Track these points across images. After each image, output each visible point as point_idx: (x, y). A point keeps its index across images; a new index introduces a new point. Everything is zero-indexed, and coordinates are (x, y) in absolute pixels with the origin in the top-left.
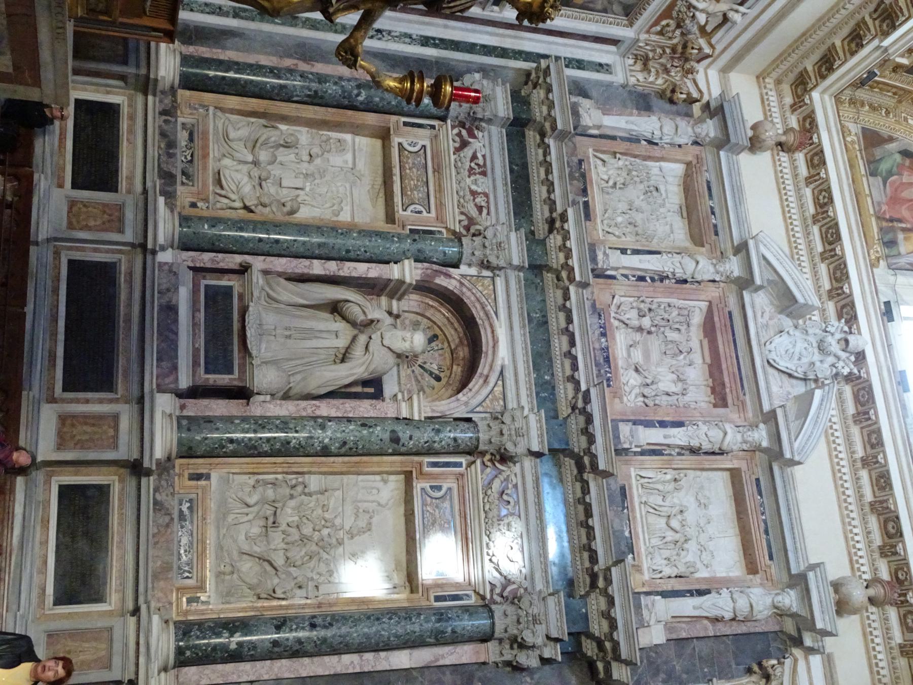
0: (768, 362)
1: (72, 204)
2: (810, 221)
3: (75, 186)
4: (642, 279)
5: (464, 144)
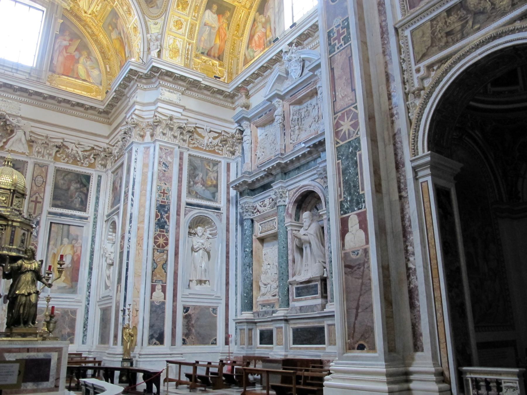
0: (300, 76)
1: (278, 344)
2: (264, 77)
3: (272, 343)
5: (258, 211)
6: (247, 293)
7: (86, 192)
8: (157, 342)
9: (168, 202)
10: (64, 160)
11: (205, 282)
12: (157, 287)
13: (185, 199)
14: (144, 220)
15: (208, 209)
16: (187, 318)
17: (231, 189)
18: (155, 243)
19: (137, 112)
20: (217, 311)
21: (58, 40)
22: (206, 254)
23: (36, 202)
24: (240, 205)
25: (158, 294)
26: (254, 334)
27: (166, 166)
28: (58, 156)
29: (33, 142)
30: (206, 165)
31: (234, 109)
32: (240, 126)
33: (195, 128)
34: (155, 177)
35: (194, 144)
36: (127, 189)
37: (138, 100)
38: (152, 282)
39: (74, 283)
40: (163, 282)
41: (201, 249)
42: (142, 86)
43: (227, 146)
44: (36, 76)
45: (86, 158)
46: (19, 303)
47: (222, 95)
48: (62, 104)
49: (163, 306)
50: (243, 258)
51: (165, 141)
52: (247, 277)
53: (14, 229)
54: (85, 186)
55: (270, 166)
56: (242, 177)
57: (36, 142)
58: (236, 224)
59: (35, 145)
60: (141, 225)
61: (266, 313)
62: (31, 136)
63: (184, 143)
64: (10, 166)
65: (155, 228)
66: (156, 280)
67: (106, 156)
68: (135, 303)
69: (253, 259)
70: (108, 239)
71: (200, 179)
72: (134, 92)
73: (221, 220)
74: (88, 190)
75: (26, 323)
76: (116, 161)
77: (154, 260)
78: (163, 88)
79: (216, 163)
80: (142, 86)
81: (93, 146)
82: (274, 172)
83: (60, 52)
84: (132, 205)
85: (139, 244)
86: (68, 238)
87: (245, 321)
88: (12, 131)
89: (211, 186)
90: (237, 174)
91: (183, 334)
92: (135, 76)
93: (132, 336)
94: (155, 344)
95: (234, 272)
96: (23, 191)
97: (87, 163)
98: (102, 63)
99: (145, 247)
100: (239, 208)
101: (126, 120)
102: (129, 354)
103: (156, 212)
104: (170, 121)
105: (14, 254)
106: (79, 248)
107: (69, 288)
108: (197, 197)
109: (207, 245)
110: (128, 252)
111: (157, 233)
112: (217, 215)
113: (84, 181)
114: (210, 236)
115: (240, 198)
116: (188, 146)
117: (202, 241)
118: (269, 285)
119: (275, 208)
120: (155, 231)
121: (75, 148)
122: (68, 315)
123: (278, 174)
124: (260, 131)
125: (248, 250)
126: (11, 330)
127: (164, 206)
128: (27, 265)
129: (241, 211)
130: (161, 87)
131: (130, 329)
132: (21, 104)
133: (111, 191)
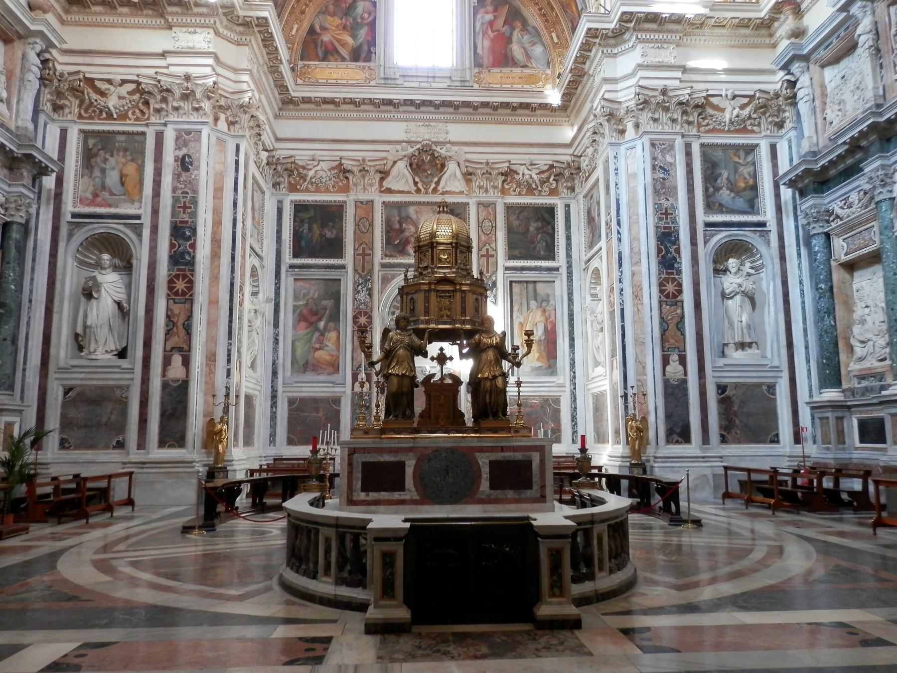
3: (884, 442)
4: (881, 66)
5: (838, 217)
6: (827, 359)
7: (551, 232)
8: (680, 440)
9: (674, 227)
10: (515, 191)
11: (750, 345)
13: (701, 217)
14: (640, 259)
15: (743, 229)
16: (725, 401)
17: (783, 188)
18: (661, 291)
19: (607, 96)
20: (775, 389)
21: (479, 16)
22: (747, 300)
23: (488, 256)
24: (802, 211)
25: (674, 368)
26: (848, 426)
27: (666, 171)
28: (506, 187)
29: (471, 174)
30: (732, 156)
31: (774, 46)
32: (789, 73)
33: (706, 98)
34: (650, 191)
35: (708, 125)
37: (607, 75)
38: (663, 351)
39: (552, 361)
41: (738, 293)
42: (609, 51)
43: (767, 115)
44: (459, 79)
45: (545, 182)
46: (484, 389)
47: (748, 27)
48: (500, 111)
49: (685, 386)
50: (816, 301)
51: (659, 130)
52: (826, 332)
53: (463, 295)
54: (549, 223)
55: (855, 132)
56: (800, 164)
57: (474, 174)
58: (798, 245)
59: (474, 178)
60: (636, 268)
61: (867, 390)
62: (467, 167)
63: (690, 127)
64: (447, 213)
65: (659, 270)
66: (669, 348)
67: (572, 174)
68: (640, 384)
69: (836, 301)
70: (592, 295)
71: (724, 180)
72: (599, 64)
75: (495, 415)
76: (587, 178)
77: (662, 318)
78: (642, 45)
79: (751, 149)
80: (609, 51)
81: (551, 163)
82: (864, 143)
83: (485, 33)
84: (620, 240)
85: (637, 296)
86: (536, 299)
87: (828, 404)
88: (443, 166)
89: (745, 189)
90: (791, 160)
91: (721, 427)
92: (597, 37)
93: (641, 431)
94: (677, 442)
95: (801, 325)
97: (547, 189)
98: (545, 32)
99: (646, 300)
100: (799, 218)
101: (594, 112)
102: (640, 457)
103: (658, 245)
104: (662, 97)
105: (468, 327)
106: (553, 312)
107: (546, 368)
108: (722, 212)
109: (748, 285)
110: (622, 310)
111: (663, 276)
112: (760, 236)
113: (546, 216)
114: (752, 271)
115: (800, 200)
116: (698, 131)
117: (739, 281)
118: (871, 343)
119: (873, 206)
120: (659, 274)
121: (527, 172)
122: (550, 405)
123: (872, 143)
124: (830, 73)
125: (823, 286)
126: (479, 423)
127: (669, 234)
129: (805, 222)
130: (639, 46)
131: (637, 421)
132: (447, 124)
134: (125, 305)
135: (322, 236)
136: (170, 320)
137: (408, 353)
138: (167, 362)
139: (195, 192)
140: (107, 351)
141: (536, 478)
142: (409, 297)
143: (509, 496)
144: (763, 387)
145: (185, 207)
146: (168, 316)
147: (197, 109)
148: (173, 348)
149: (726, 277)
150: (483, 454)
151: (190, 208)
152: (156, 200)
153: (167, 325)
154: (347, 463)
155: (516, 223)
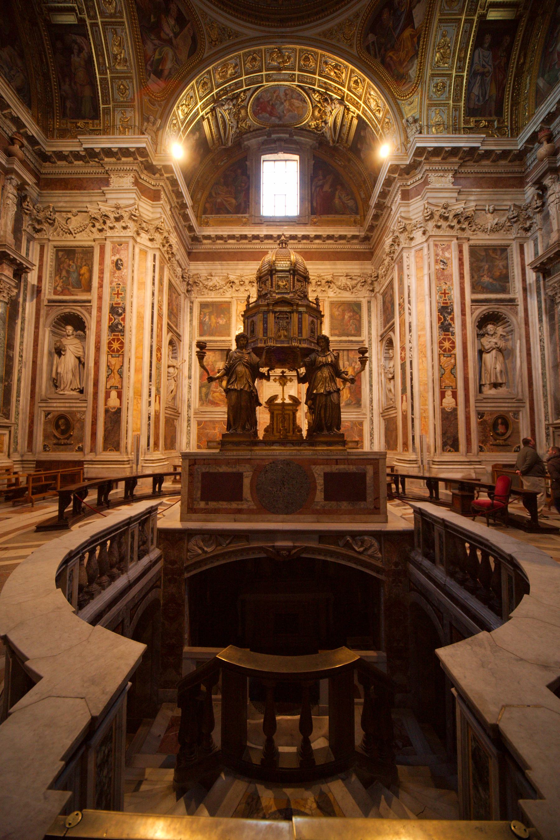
8: (452, 449)
11: (500, 385)
12: (446, 393)
18: (441, 347)
19: (403, 215)
20: (518, 415)
34: (433, 277)
36: (402, 300)
40: (453, 387)
53: (300, 316)
54: (357, 313)
73: (517, 313)
74: (360, 317)
75: (330, 429)
84: (410, 314)
94: (449, 451)
96: (304, 273)
105: (305, 345)
109: (501, 344)
111: (442, 337)
112: (511, 309)
113: (355, 308)
117: (495, 340)
122: (357, 426)
127: (447, 308)
128: (321, 359)
133: (382, 313)
134: (82, 359)
135: (217, 323)
136: (109, 368)
137: (247, 370)
138: (108, 395)
139: (125, 283)
140: (72, 389)
141: (370, 490)
142: (250, 321)
143: (343, 507)
144: (510, 414)
145: (118, 294)
146: (108, 366)
147: (125, 228)
148: (111, 387)
149: (485, 338)
150: (318, 466)
151: (121, 294)
152: (100, 290)
153: (107, 372)
154: (187, 473)
155: (337, 313)
